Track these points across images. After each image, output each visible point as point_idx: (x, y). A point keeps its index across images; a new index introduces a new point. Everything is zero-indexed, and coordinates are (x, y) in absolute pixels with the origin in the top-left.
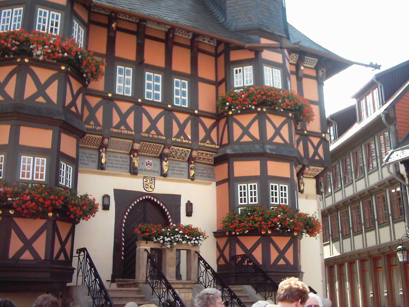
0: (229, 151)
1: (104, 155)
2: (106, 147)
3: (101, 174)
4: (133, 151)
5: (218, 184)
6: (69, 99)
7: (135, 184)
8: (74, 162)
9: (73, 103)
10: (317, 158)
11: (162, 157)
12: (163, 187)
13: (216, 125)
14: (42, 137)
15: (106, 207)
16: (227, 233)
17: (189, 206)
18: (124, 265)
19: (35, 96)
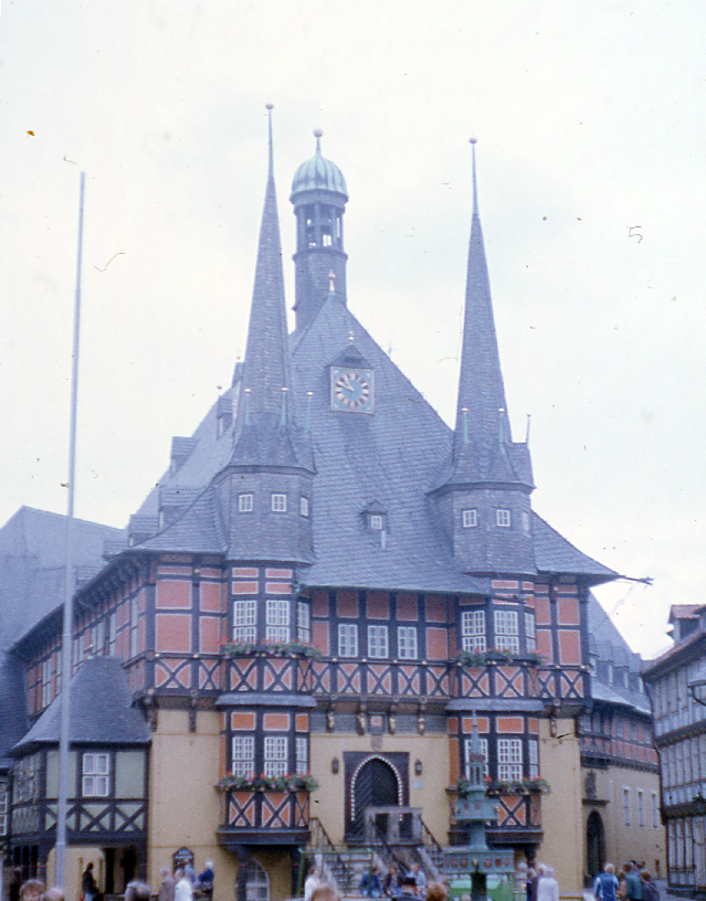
0: (457, 708)
1: (331, 718)
2: (333, 710)
3: (329, 737)
4: (358, 712)
5: (451, 736)
6: (300, 681)
7: (363, 744)
8: (307, 735)
9: (304, 684)
10: (573, 696)
11: (389, 713)
12: (390, 744)
13: (447, 673)
14: (283, 722)
15: (335, 771)
16: (458, 793)
17: (418, 763)
18: (353, 828)
19: (273, 685)
